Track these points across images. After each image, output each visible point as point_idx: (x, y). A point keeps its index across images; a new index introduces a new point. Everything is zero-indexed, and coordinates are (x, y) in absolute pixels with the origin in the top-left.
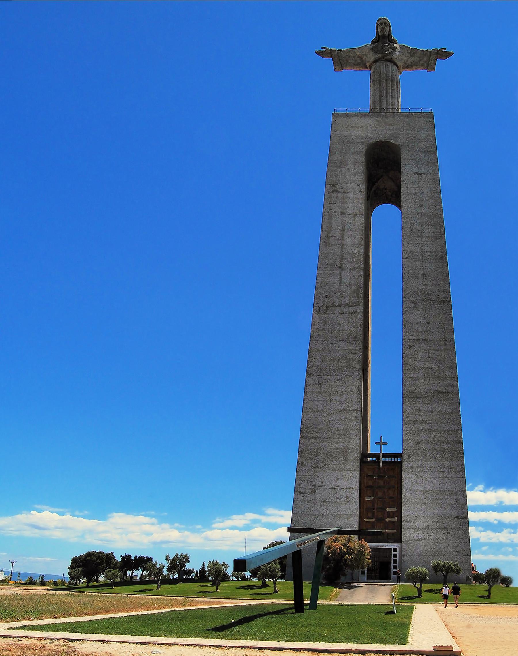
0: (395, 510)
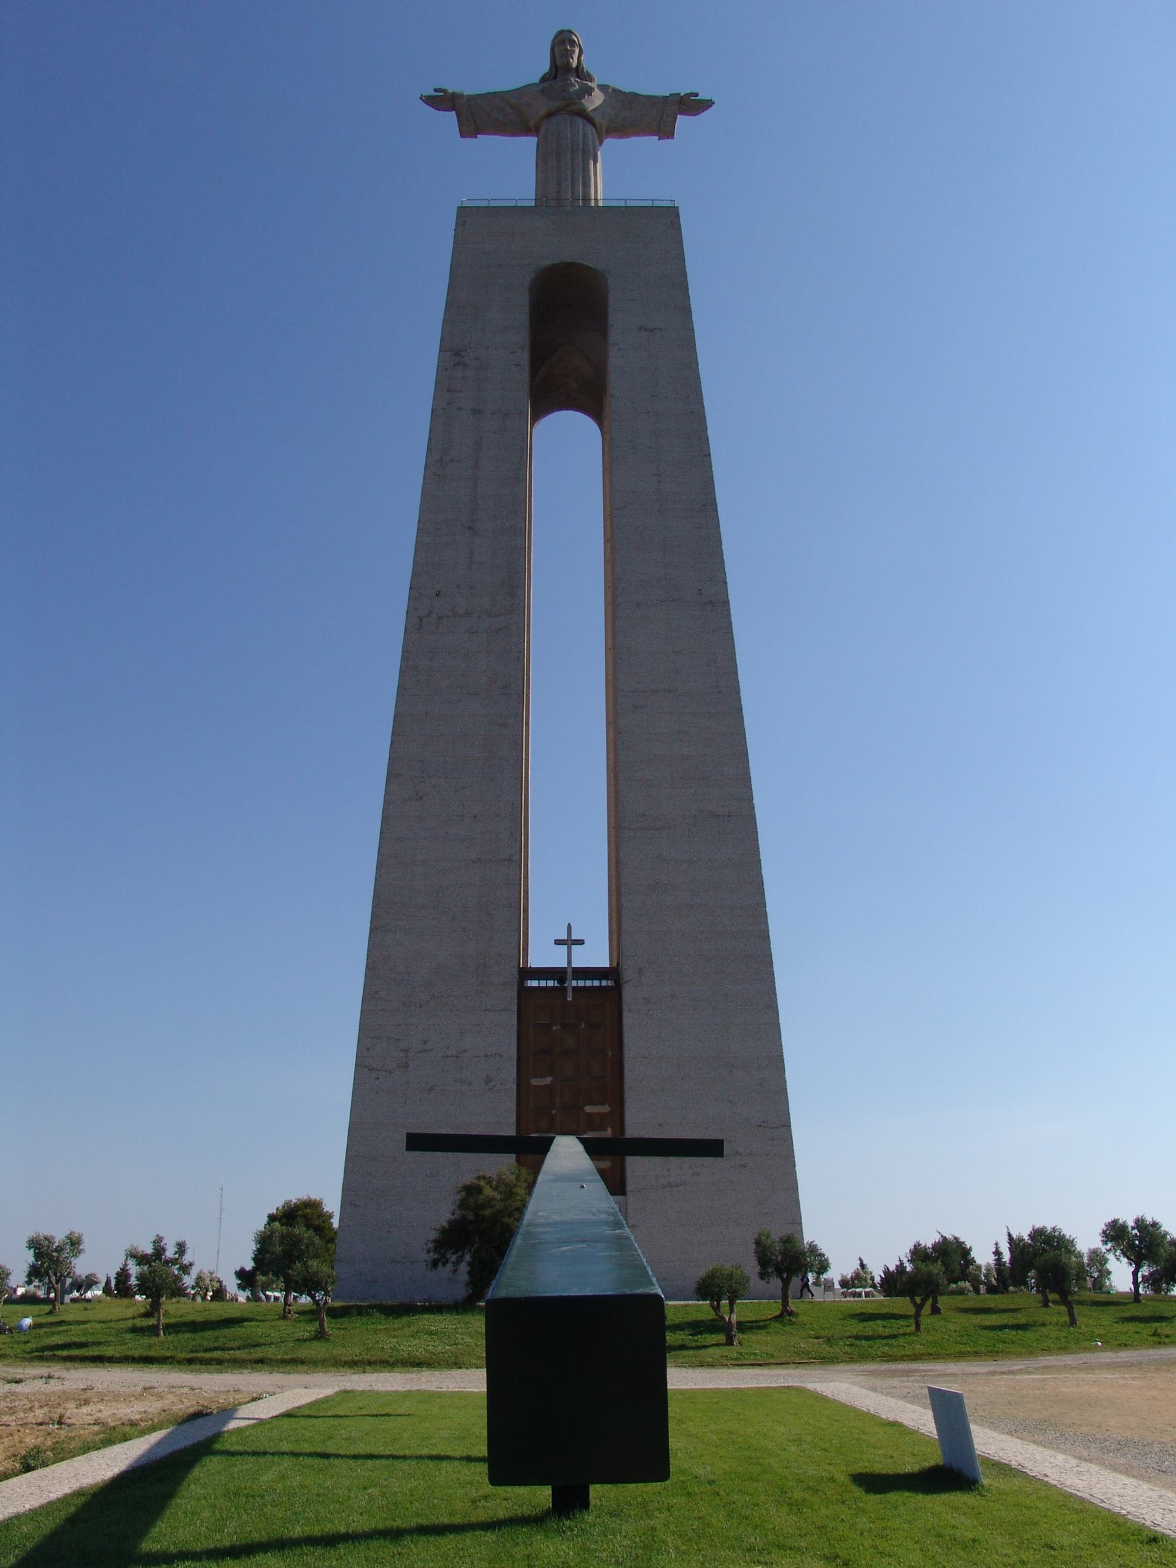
0: (605, 1109)
